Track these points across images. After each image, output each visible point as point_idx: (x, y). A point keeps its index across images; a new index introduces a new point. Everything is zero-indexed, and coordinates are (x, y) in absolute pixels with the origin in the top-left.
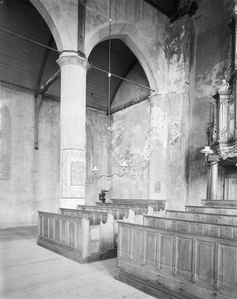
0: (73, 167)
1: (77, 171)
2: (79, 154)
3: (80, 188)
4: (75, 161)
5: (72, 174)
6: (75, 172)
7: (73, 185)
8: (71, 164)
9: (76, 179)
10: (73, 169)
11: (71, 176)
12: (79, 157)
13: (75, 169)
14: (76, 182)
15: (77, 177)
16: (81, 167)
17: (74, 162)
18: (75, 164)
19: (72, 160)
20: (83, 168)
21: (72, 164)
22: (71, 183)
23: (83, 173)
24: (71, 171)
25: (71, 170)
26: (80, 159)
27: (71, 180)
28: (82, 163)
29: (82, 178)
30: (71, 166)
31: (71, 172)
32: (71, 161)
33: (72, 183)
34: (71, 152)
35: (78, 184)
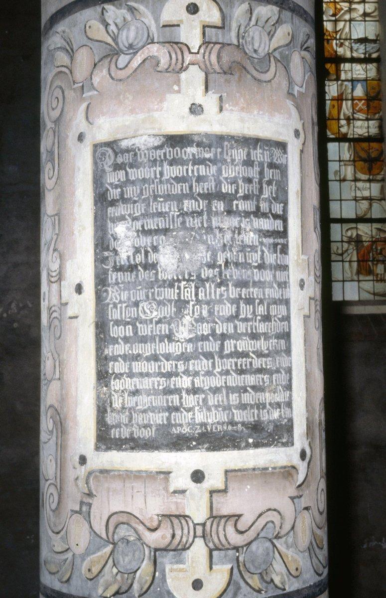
0: (121, 210)
1: (167, 260)
2: (195, 42)
3: (214, 480)
4: (144, 141)
5: (113, 294)
6: (143, 275)
7: (119, 444)
8: (98, 179)
9: (155, 358)
10: (125, 237)
11: (101, 327)
12: (194, 77)
13: (145, 241)
14: (160, 401)
15: (170, 337)
16: (220, 206)
17: (133, 151)
18: (144, 172)
19: (105, 128)
20: (258, 213)
21: (113, 178)
22: (102, 411)
23: (267, 276)
24: (100, 260)
25: (103, 244)
26: (210, 102)
27: (103, 376)
28: (240, 154)
29: (243, 345)
30: (102, 200)
31: (101, 281)
32: (96, 146)
33: (110, 419)
34: (98, 31)
35: (197, 415)
